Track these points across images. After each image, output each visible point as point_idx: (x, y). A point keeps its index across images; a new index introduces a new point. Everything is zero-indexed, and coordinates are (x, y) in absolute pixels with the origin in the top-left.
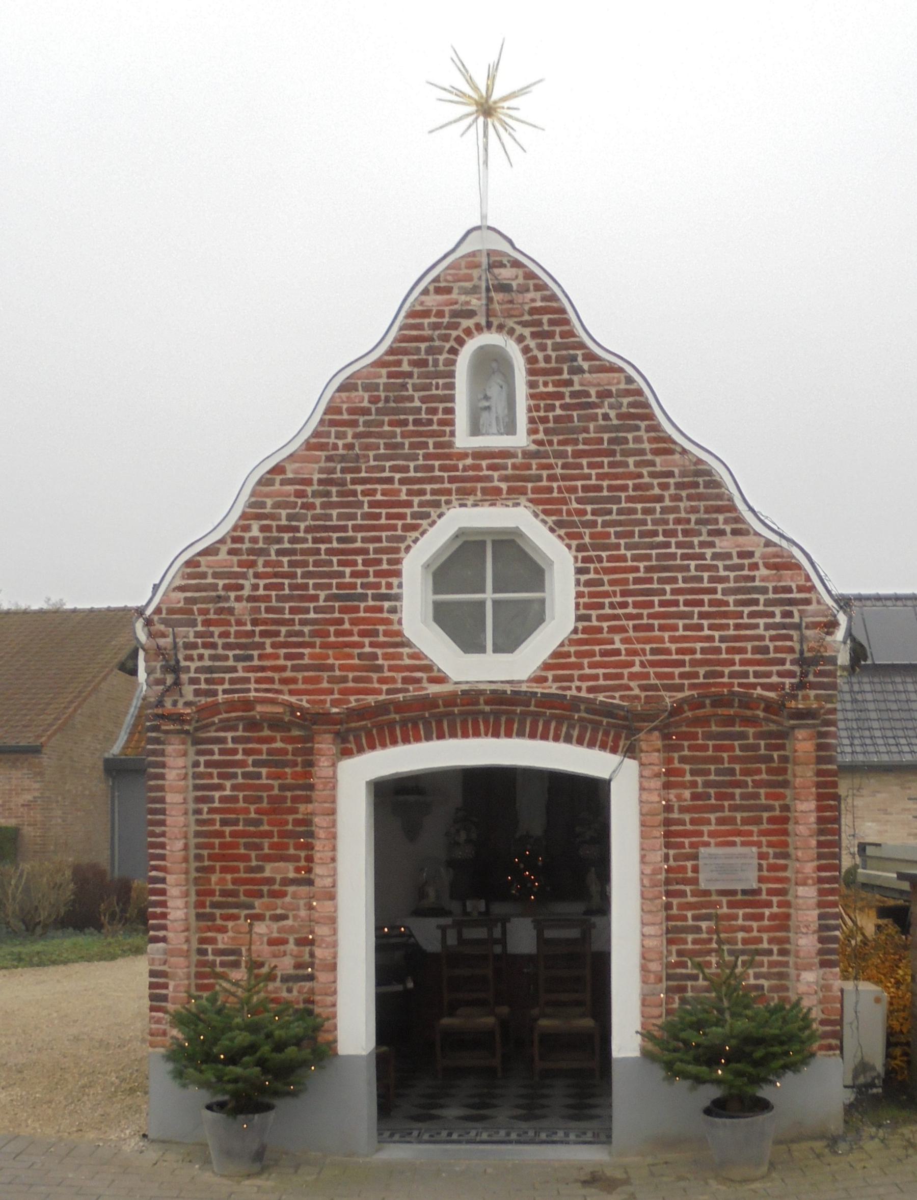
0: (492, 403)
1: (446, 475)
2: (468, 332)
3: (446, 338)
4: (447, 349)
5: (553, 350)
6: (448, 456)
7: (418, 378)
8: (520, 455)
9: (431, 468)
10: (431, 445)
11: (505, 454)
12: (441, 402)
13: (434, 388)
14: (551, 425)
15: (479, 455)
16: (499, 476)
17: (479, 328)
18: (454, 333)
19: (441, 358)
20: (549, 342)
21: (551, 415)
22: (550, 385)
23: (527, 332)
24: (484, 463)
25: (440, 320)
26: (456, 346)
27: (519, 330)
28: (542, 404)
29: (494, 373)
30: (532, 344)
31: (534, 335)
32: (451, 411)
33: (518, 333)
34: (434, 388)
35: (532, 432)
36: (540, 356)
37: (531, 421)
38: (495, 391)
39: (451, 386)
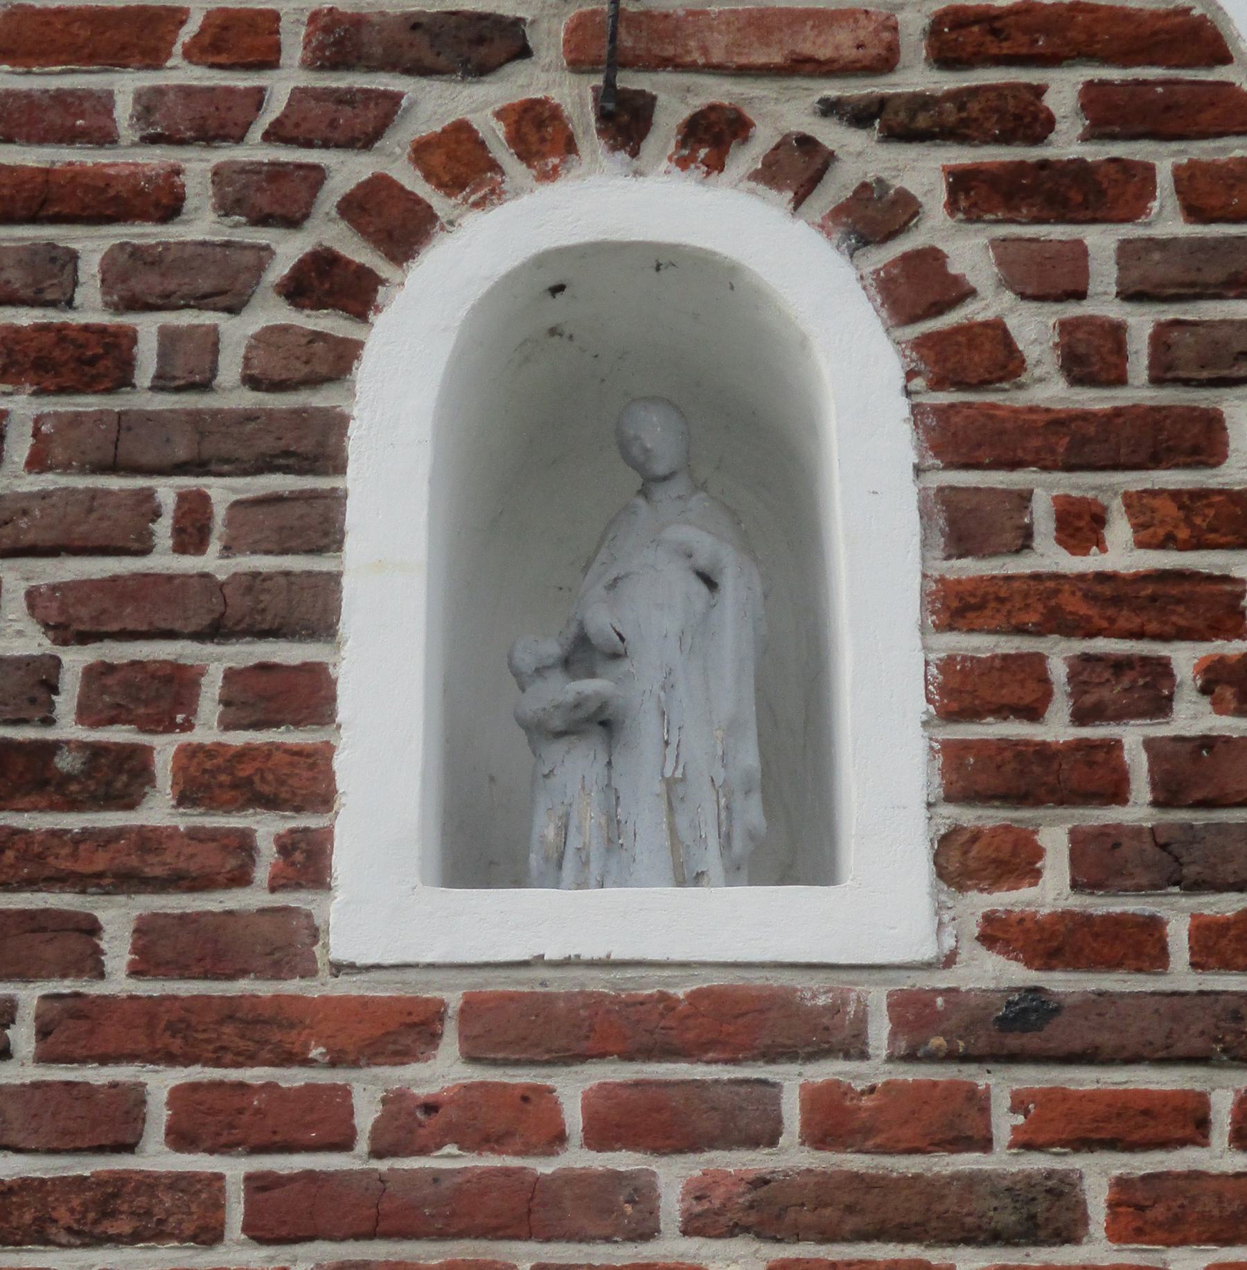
0: (636, 687)
1: (234, 1169)
2: (461, 164)
3: (275, 199)
4: (279, 269)
5: (1131, 295)
6: (266, 1033)
7: (37, 463)
8: (879, 1032)
9: (117, 1122)
10: (117, 949)
11: (750, 1018)
12: (216, 632)
13: (163, 529)
14: (1138, 811)
15: (529, 1020)
16: (698, 1192)
17: (539, 136)
18: (347, 170)
19: (237, 332)
20: (1102, 241)
21: (1132, 738)
22: (1119, 531)
23: (922, 171)
24: (572, 1089)
25: (242, 81)
26: (358, 251)
27: (860, 157)
28: (1059, 655)
29: (649, 484)
30: (969, 251)
31: (971, 193)
32: (309, 696)
33: (838, 186)
34: (163, 529)
35: (963, 862)
36: (1034, 329)
37: (969, 776)
38: (652, 607)
39: (320, 526)
